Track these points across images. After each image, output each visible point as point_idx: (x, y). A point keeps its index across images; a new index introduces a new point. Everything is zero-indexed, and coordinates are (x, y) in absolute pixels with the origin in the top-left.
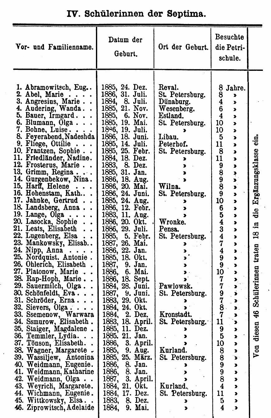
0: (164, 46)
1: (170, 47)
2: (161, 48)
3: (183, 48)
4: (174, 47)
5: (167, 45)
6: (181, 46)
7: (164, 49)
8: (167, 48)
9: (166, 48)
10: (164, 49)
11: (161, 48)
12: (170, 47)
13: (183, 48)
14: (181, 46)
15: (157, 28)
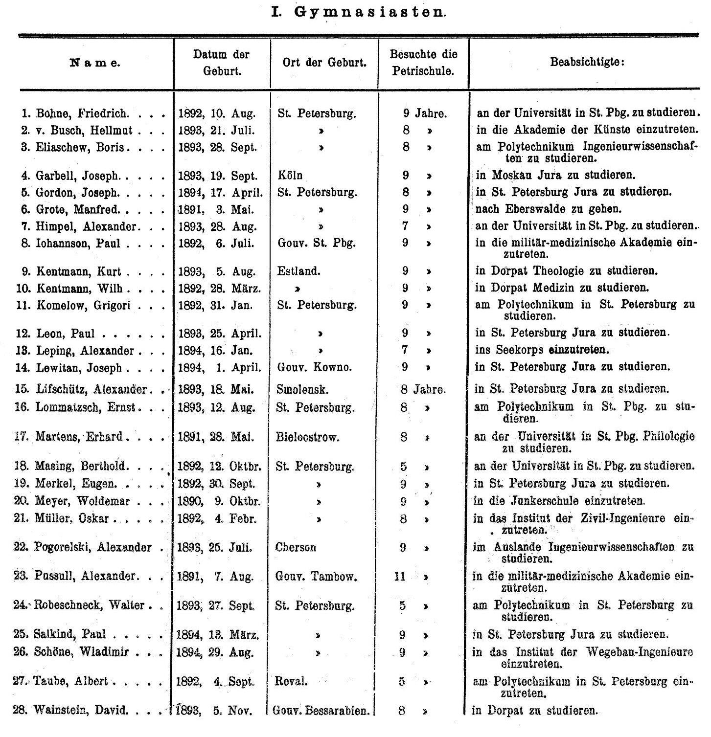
0: (293, 61)
1: (303, 62)
2: (287, 63)
3: (325, 64)
4: (309, 63)
5: (298, 61)
6: (320, 61)
7: (293, 66)
8: (298, 65)
9: (295, 64)
10: (293, 66)
11: (287, 63)
12: (303, 62)
13: (325, 64)
14: (320, 61)
15: (275, 41)
